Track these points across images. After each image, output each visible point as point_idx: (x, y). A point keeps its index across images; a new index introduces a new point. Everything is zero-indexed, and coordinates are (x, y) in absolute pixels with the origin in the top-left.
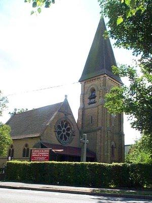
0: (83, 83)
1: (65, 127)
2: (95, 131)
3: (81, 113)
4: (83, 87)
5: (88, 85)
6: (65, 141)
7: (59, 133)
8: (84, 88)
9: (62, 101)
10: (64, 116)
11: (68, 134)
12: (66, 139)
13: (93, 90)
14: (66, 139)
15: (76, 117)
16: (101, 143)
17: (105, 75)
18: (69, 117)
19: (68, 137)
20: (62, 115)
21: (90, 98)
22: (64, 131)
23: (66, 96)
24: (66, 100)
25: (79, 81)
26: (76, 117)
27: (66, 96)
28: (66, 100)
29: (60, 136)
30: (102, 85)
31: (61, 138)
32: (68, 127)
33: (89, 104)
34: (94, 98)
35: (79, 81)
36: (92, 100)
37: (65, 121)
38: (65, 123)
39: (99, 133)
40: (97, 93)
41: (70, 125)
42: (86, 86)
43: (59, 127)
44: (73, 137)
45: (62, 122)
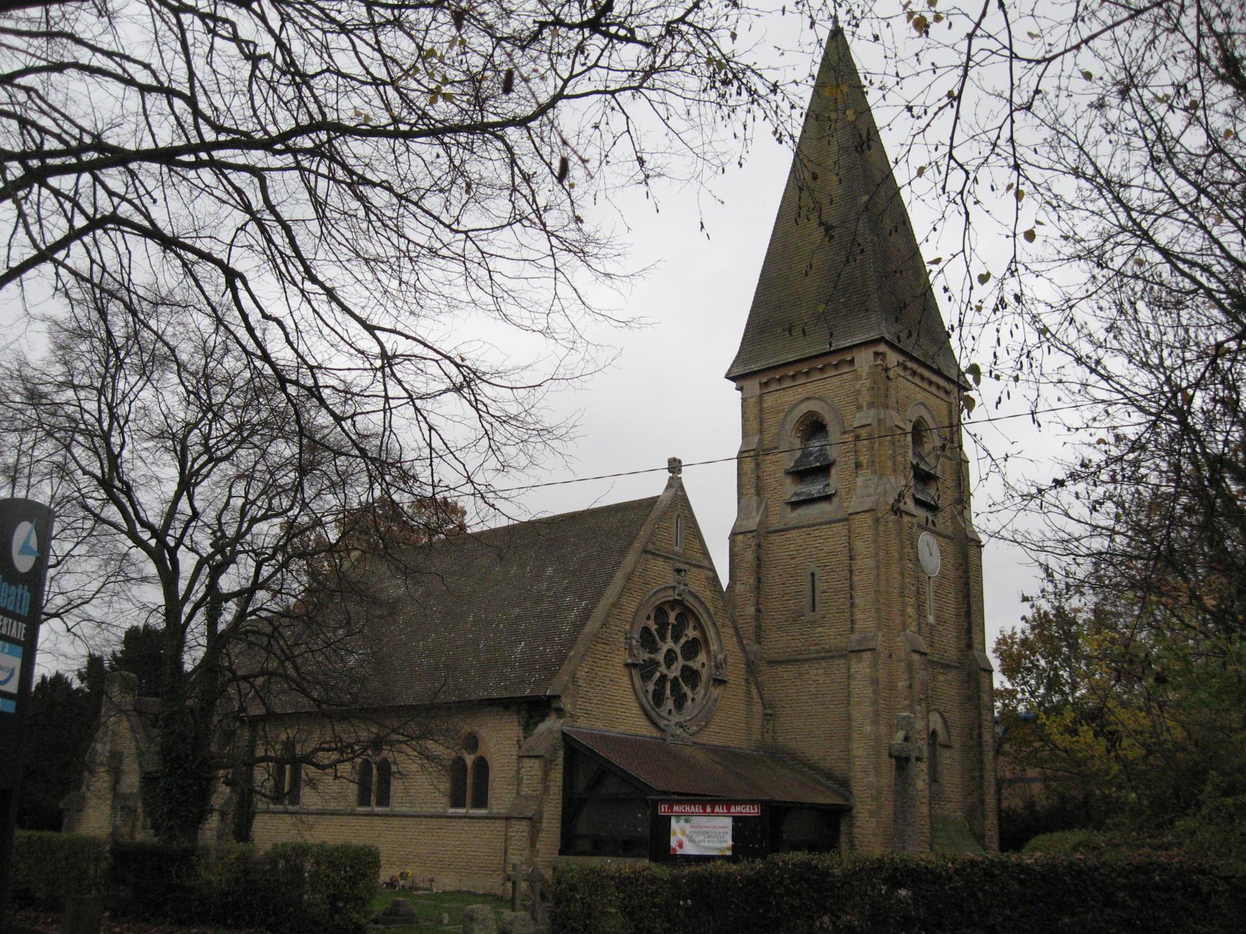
0: (753, 385)
1: (676, 638)
2: (829, 655)
3: (749, 556)
4: (753, 411)
5: (794, 399)
6: (675, 718)
7: (646, 670)
8: (753, 419)
9: (654, 486)
10: (671, 579)
11: (691, 676)
12: (680, 701)
14: (680, 701)
15: (724, 581)
17: (882, 348)
18: (695, 580)
19: (690, 694)
20: (661, 572)
21: (801, 474)
22: (670, 658)
23: (675, 466)
24: (675, 485)
26: (724, 581)
27: (675, 466)
28: (675, 485)
30: (865, 398)
31: (658, 698)
32: (691, 633)
33: (795, 505)
34: (824, 470)
36: (815, 489)
37: (674, 604)
38: (672, 618)
39: (862, 667)
40: (836, 446)
41: (699, 626)
42: (769, 401)
43: (648, 640)
44: (716, 692)
45: (660, 612)
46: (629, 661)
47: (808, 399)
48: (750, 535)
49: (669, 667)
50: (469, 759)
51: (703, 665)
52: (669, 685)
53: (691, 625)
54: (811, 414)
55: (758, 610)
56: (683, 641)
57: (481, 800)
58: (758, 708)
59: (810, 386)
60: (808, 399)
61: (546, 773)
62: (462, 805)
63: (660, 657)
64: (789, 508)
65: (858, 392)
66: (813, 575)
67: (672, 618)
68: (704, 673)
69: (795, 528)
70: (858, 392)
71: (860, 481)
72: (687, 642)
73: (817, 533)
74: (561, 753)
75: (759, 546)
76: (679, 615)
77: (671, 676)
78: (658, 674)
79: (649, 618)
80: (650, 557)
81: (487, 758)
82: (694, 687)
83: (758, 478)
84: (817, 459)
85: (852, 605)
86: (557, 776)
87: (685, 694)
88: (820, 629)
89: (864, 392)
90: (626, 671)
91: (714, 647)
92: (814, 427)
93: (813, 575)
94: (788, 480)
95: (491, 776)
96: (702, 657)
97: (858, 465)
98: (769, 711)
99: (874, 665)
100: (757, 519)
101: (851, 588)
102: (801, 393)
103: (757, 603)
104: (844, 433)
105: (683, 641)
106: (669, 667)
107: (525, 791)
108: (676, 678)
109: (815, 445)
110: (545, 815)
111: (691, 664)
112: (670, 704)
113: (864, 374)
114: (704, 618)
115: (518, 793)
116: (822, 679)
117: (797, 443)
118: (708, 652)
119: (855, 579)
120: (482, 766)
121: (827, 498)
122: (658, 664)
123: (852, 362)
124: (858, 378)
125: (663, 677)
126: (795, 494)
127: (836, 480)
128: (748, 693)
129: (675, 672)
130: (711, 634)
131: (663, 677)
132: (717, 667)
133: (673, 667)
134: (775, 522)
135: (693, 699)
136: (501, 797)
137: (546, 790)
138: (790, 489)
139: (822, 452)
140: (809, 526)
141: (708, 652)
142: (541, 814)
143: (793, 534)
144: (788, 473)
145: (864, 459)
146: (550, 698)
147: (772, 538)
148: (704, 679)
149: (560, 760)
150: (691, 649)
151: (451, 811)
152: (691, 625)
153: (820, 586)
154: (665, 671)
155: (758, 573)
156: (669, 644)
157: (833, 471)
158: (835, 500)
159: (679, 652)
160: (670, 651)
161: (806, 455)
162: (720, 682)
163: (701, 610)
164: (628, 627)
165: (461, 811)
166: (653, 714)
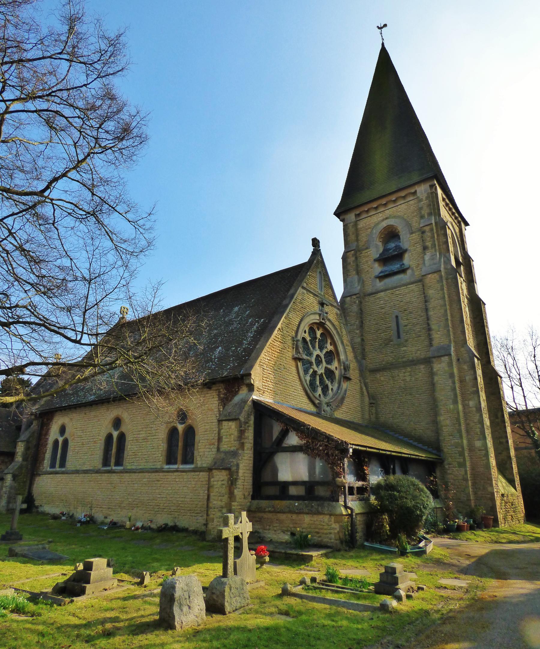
1: (321, 348)
11: (330, 374)
12: (325, 389)
13: (391, 235)
14: (325, 389)
16: (455, 402)
19: (330, 387)
21: (384, 260)
23: (315, 242)
25: (338, 214)
27: (315, 242)
29: (308, 378)
30: (425, 211)
33: (381, 277)
34: (399, 255)
35: (338, 214)
36: (395, 267)
38: (319, 333)
41: (333, 343)
44: (345, 385)
46: (296, 356)
47: (387, 218)
48: (355, 297)
49: (318, 366)
50: (181, 428)
51: (336, 368)
52: (318, 378)
53: (329, 341)
54: (389, 227)
55: (363, 340)
56: (324, 351)
57: (188, 458)
58: (367, 399)
59: (387, 212)
60: (387, 218)
61: (242, 433)
62: (176, 463)
63: (313, 360)
64: (378, 280)
65: (421, 209)
66: (397, 317)
67: (319, 333)
68: (337, 373)
69: (382, 291)
70: (421, 209)
71: (427, 257)
72: (327, 352)
73: (397, 292)
74: (252, 418)
75: (361, 302)
76: (321, 334)
77: (319, 372)
78: (311, 371)
79: (305, 332)
80: (305, 292)
81: (194, 426)
82: (332, 383)
83: (357, 265)
84: (394, 251)
85: (430, 329)
86: (250, 434)
87: (327, 386)
88: (405, 348)
89: (425, 208)
90: (293, 363)
91: (342, 357)
92: (391, 235)
93: (397, 317)
94: (376, 265)
95: (197, 438)
96: (335, 364)
97: (425, 248)
98: (374, 402)
99: (450, 364)
100: (359, 287)
101: (428, 319)
102: (381, 216)
103: (362, 335)
104: (412, 233)
105: (324, 351)
106: (318, 366)
107: (225, 447)
108: (322, 374)
109: (392, 245)
110: (241, 466)
111: (329, 366)
112: (319, 391)
113: (424, 198)
114: (336, 338)
115: (218, 449)
116: (408, 379)
117: (380, 244)
118: (339, 360)
119: (431, 313)
120: (190, 432)
121: (403, 271)
122: (311, 363)
123: (415, 193)
124: (420, 200)
125: (315, 372)
126: (381, 272)
127: (407, 260)
128: (361, 388)
129: (321, 370)
130: (340, 348)
131: (315, 372)
132: (345, 369)
133: (320, 367)
134: (369, 289)
135: (332, 389)
136: (204, 453)
137: (242, 445)
138: (378, 269)
139: (398, 247)
140: (392, 288)
141: (339, 360)
142: (238, 465)
143: (382, 294)
144: (375, 260)
145: (429, 244)
146: (243, 376)
147: (367, 299)
148: (337, 377)
149: (252, 422)
150: (330, 356)
151: (167, 467)
152: (329, 341)
153: (402, 322)
154: (316, 369)
155: (361, 318)
156: (317, 352)
157: (406, 256)
158: (409, 272)
159: (323, 357)
160: (318, 356)
161: (385, 250)
162: (348, 379)
163: (335, 332)
164: (294, 334)
165: (175, 467)
166: (311, 395)
